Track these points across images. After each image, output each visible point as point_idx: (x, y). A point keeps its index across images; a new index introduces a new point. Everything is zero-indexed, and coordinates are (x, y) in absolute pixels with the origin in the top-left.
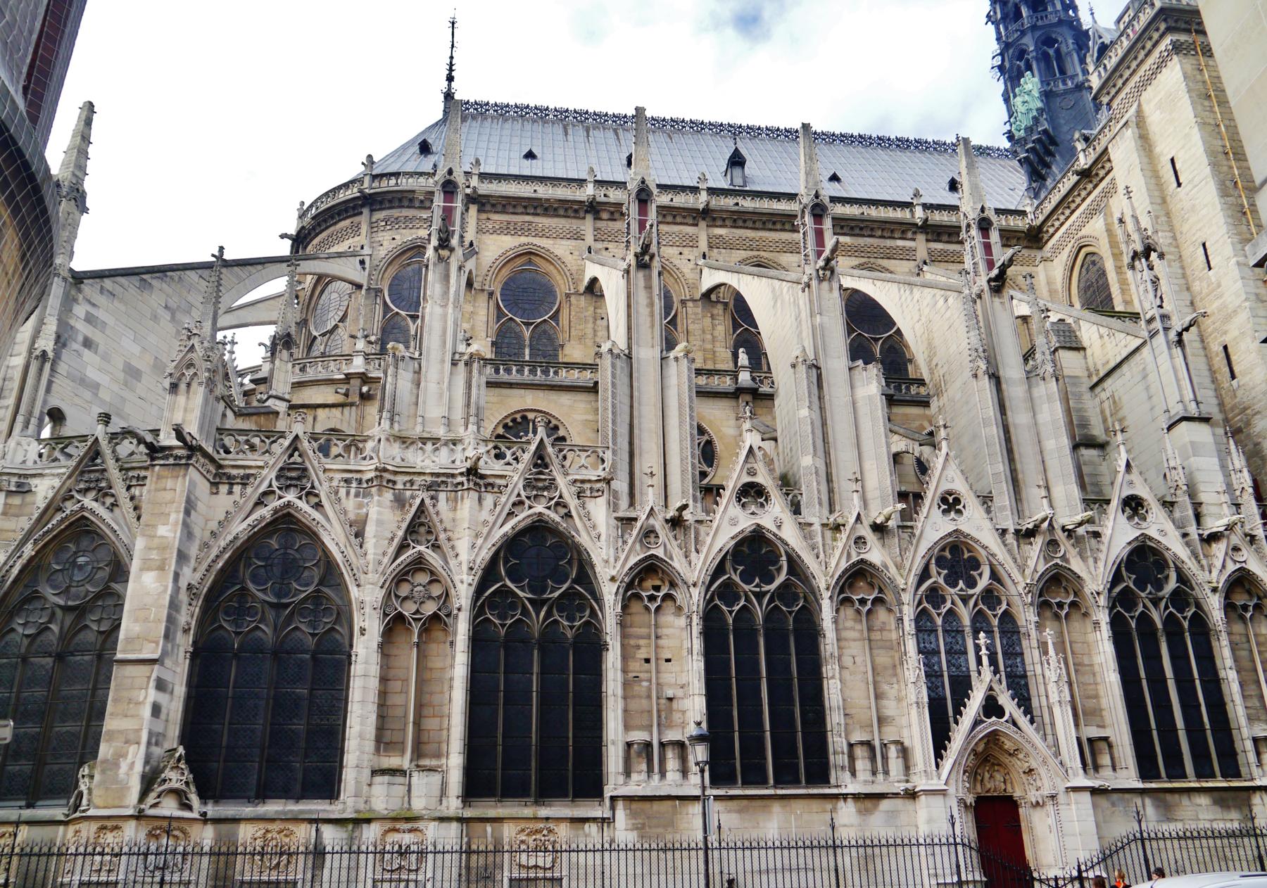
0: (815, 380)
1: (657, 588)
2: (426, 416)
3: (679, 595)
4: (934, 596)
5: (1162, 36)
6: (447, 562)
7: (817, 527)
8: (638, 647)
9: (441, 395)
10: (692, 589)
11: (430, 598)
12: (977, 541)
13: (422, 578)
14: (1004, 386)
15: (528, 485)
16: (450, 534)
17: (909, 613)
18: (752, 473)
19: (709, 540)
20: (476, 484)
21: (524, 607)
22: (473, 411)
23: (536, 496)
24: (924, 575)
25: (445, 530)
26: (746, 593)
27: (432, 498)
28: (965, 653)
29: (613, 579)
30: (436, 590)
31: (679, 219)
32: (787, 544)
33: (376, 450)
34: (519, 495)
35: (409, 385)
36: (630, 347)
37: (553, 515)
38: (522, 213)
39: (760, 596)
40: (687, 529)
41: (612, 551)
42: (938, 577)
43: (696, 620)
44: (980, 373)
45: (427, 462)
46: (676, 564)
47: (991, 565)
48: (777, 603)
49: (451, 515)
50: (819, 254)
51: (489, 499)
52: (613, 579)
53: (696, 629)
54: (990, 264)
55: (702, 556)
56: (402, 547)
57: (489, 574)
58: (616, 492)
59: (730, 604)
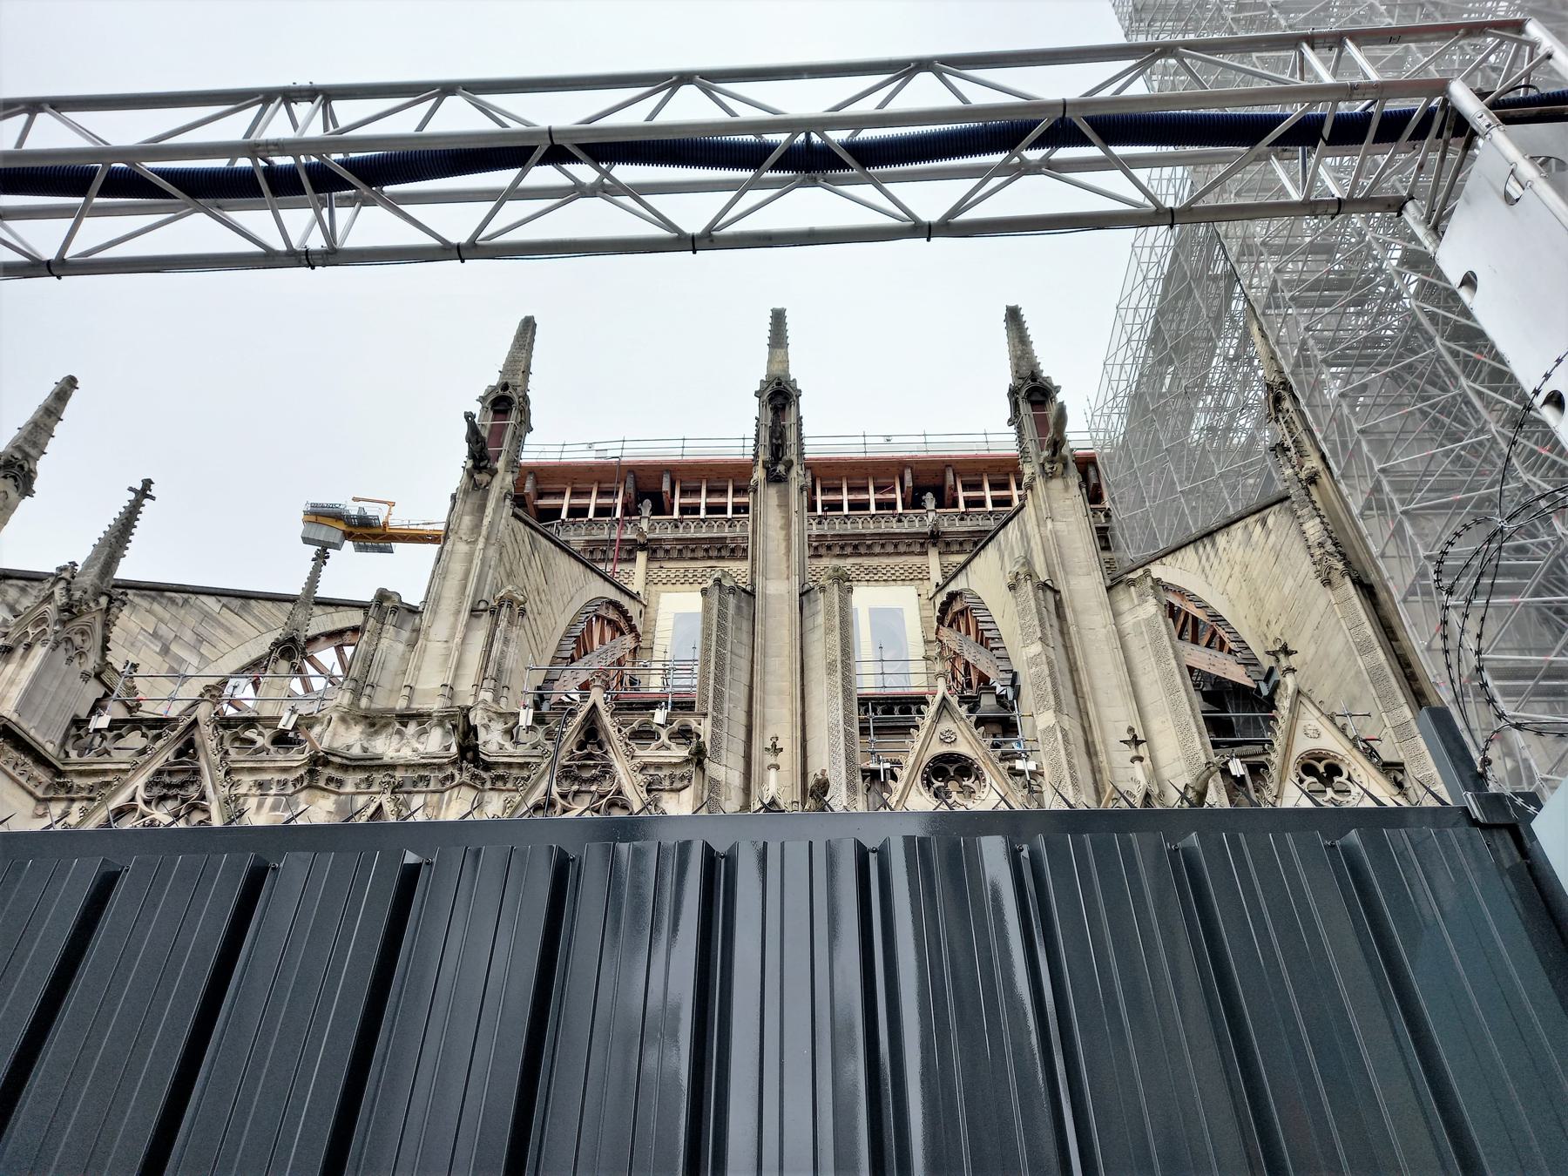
20: (474, 777)
22: (491, 671)
23: (576, 793)
31: (902, 548)
33: (320, 736)
38: (703, 558)
44: (1335, 576)
58: (714, 785)
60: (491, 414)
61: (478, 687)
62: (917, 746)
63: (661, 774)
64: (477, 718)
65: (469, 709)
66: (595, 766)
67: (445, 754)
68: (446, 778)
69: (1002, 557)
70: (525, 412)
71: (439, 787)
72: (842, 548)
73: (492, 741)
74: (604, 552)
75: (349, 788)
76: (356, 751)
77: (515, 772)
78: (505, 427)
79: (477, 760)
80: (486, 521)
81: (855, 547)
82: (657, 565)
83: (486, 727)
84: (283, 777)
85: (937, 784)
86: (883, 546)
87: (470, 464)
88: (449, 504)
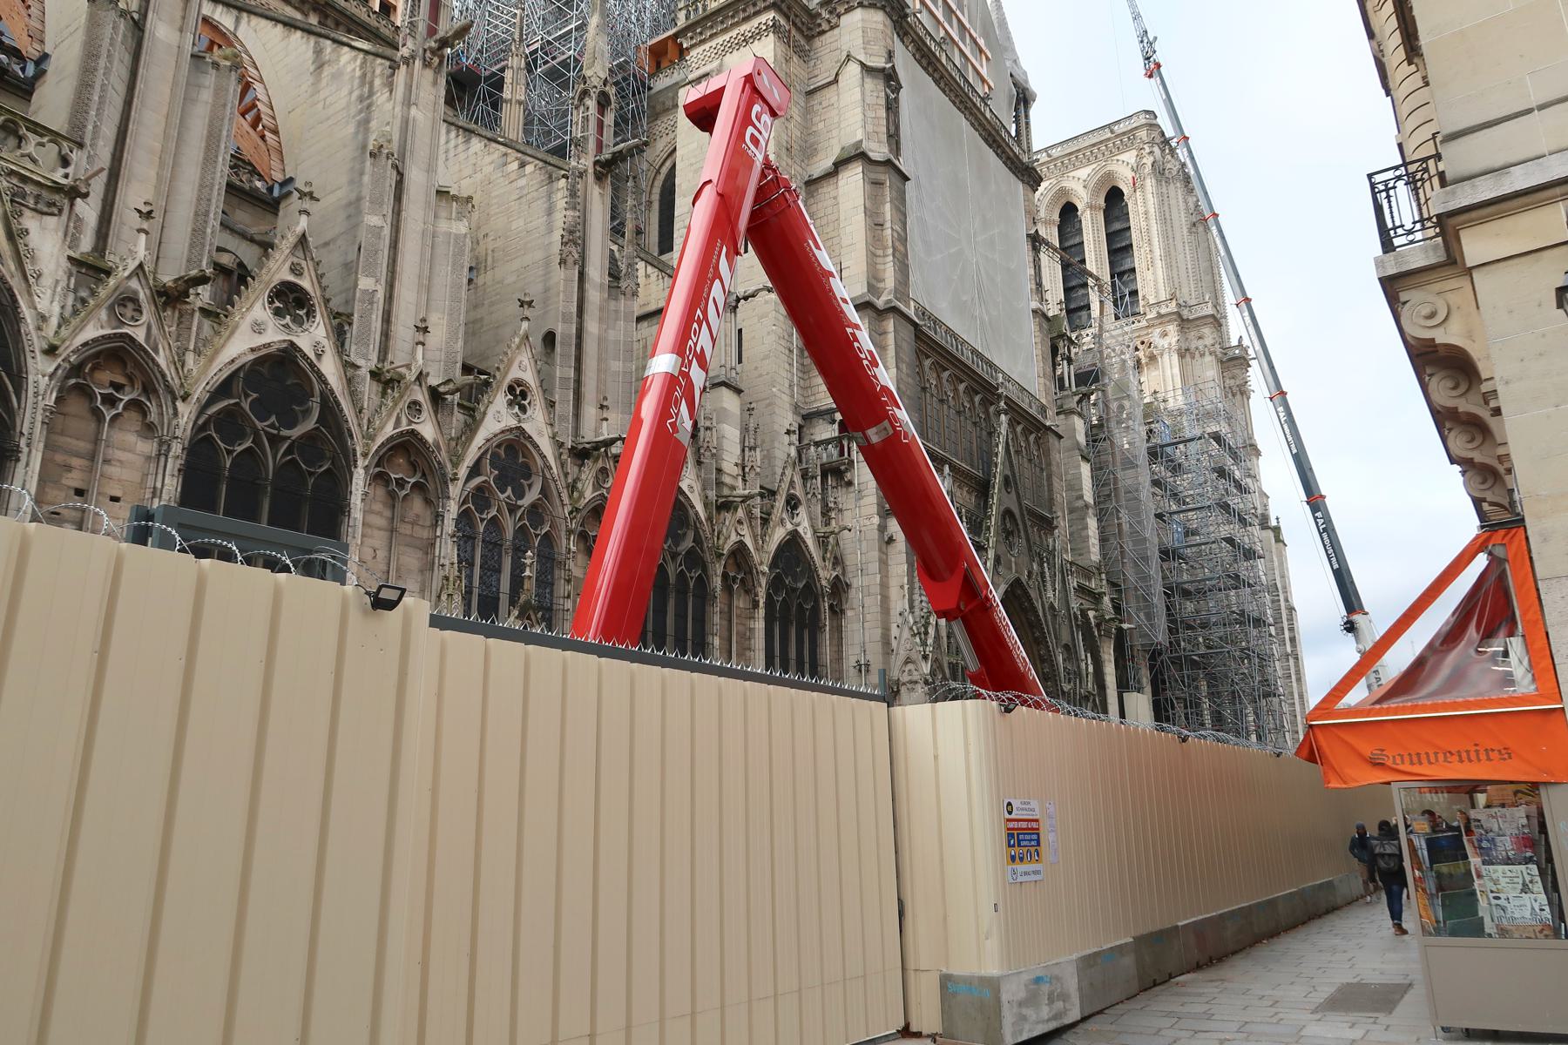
1: (118, 387)
4: (480, 497)
5: (766, 9)
7: (364, 372)
8: (69, 468)
10: (179, 404)
12: (536, 446)
17: (452, 510)
18: (296, 270)
24: (475, 470)
26: (256, 432)
28: (499, 571)
29: (51, 351)
32: (325, 382)
36: (145, 16)
39: (275, 441)
41: (56, 309)
42: (489, 475)
43: (177, 448)
46: (161, 360)
47: (544, 477)
50: (432, 31)
53: (173, 465)
58: (79, 219)
59: (230, 441)
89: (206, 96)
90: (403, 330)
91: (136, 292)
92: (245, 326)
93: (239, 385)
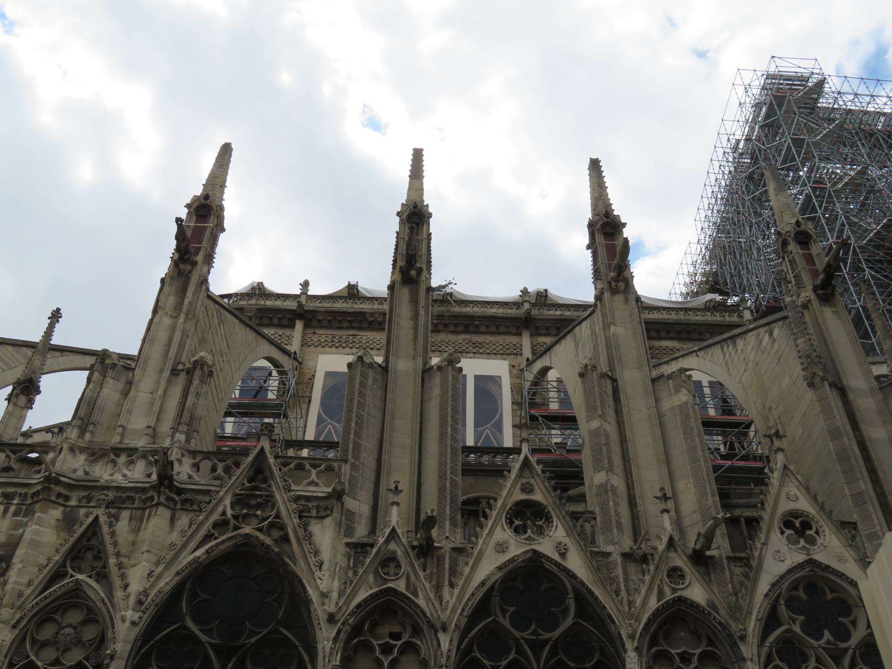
0: (610, 391)
1: (396, 636)
2: (130, 427)
3: (425, 646)
6: (110, 593)
7: (617, 558)
9: (152, 405)
11: (79, 642)
12: (841, 575)
13: (74, 617)
14: (851, 396)
15: (238, 501)
16: (124, 560)
19: (467, 570)
20: (169, 499)
21: (207, 657)
22: (186, 418)
24: (771, 621)
25: (118, 555)
27: (109, 515)
30: (90, 633)
31: (502, 329)
32: (573, 576)
33: (53, 461)
34: (224, 513)
35: (117, 396)
37: (262, 537)
38: (347, 328)
40: (441, 559)
41: (336, 584)
44: (817, 380)
45: (118, 477)
46: (421, 602)
48: (562, 656)
49: (131, 537)
51: (184, 520)
52: (331, 619)
54: (814, 273)
55: (457, 591)
56: (57, 575)
57: (166, 611)
58: (350, 516)
60: (194, 218)
61: (175, 430)
62: (504, 493)
63: (310, 505)
64: (174, 455)
65: (168, 449)
66: (261, 496)
67: (148, 480)
68: (147, 499)
69: (577, 347)
70: (220, 218)
71: (142, 505)
72: (456, 326)
73: (183, 471)
74: (270, 319)
75: (73, 503)
76: (80, 474)
77: (199, 498)
78: (205, 228)
79: (171, 487)
80: (187, 301)
81: (466, 326)
82: (311, 331)
83: (180, 461)
84: (24, 491)
85: (517, 523)
86: (487, 326)
87: (177, 256)
88: (159, 285)
89: (436, 392)
90: (650, 507)
91: (394, 552)
92: (490, 549)
93: (496, 600)
